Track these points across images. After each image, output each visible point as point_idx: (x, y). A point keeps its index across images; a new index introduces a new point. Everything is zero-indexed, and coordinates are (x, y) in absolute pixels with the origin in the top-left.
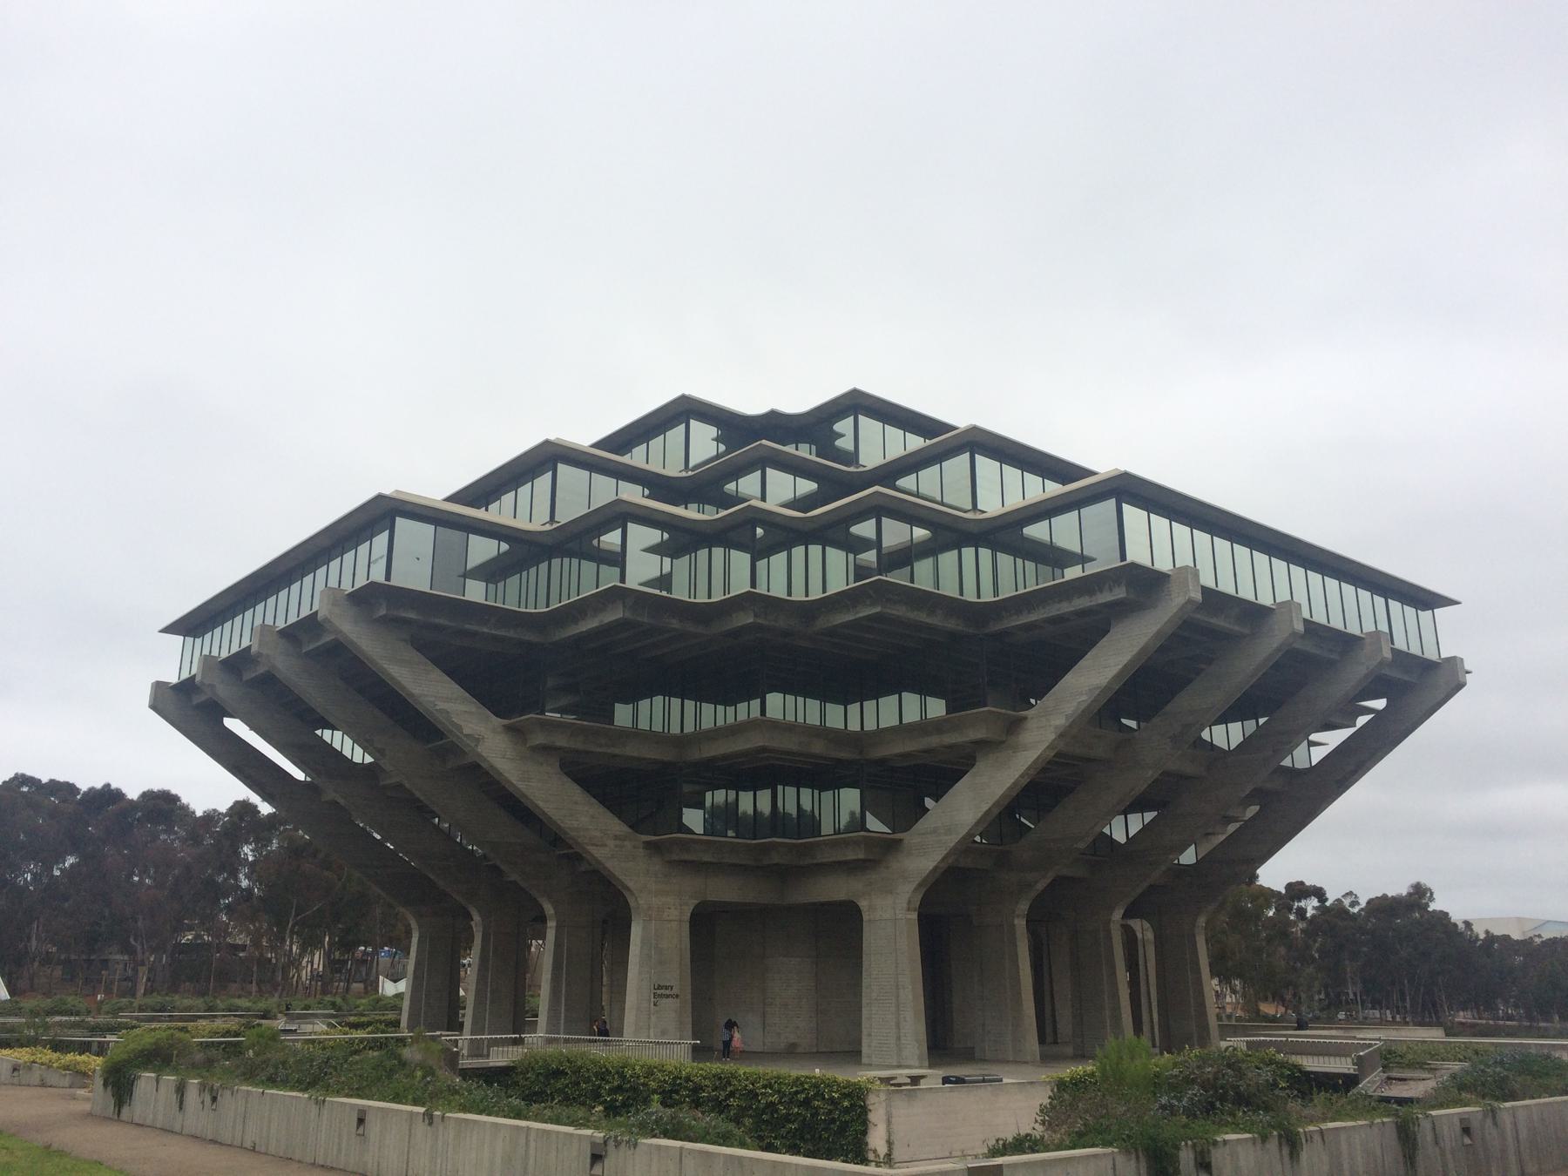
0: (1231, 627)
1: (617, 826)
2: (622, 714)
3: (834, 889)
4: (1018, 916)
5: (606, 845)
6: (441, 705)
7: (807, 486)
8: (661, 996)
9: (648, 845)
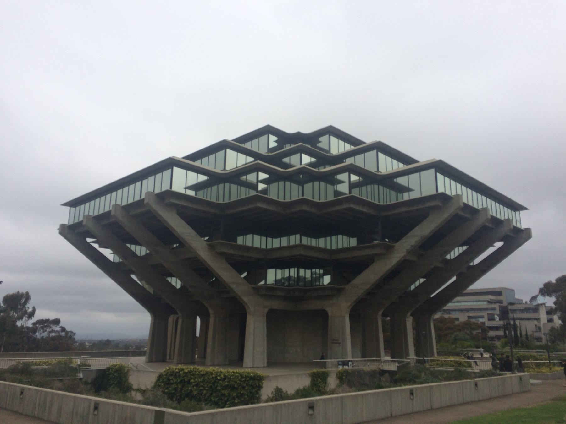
2: (240, 240)
7: (313, 160)
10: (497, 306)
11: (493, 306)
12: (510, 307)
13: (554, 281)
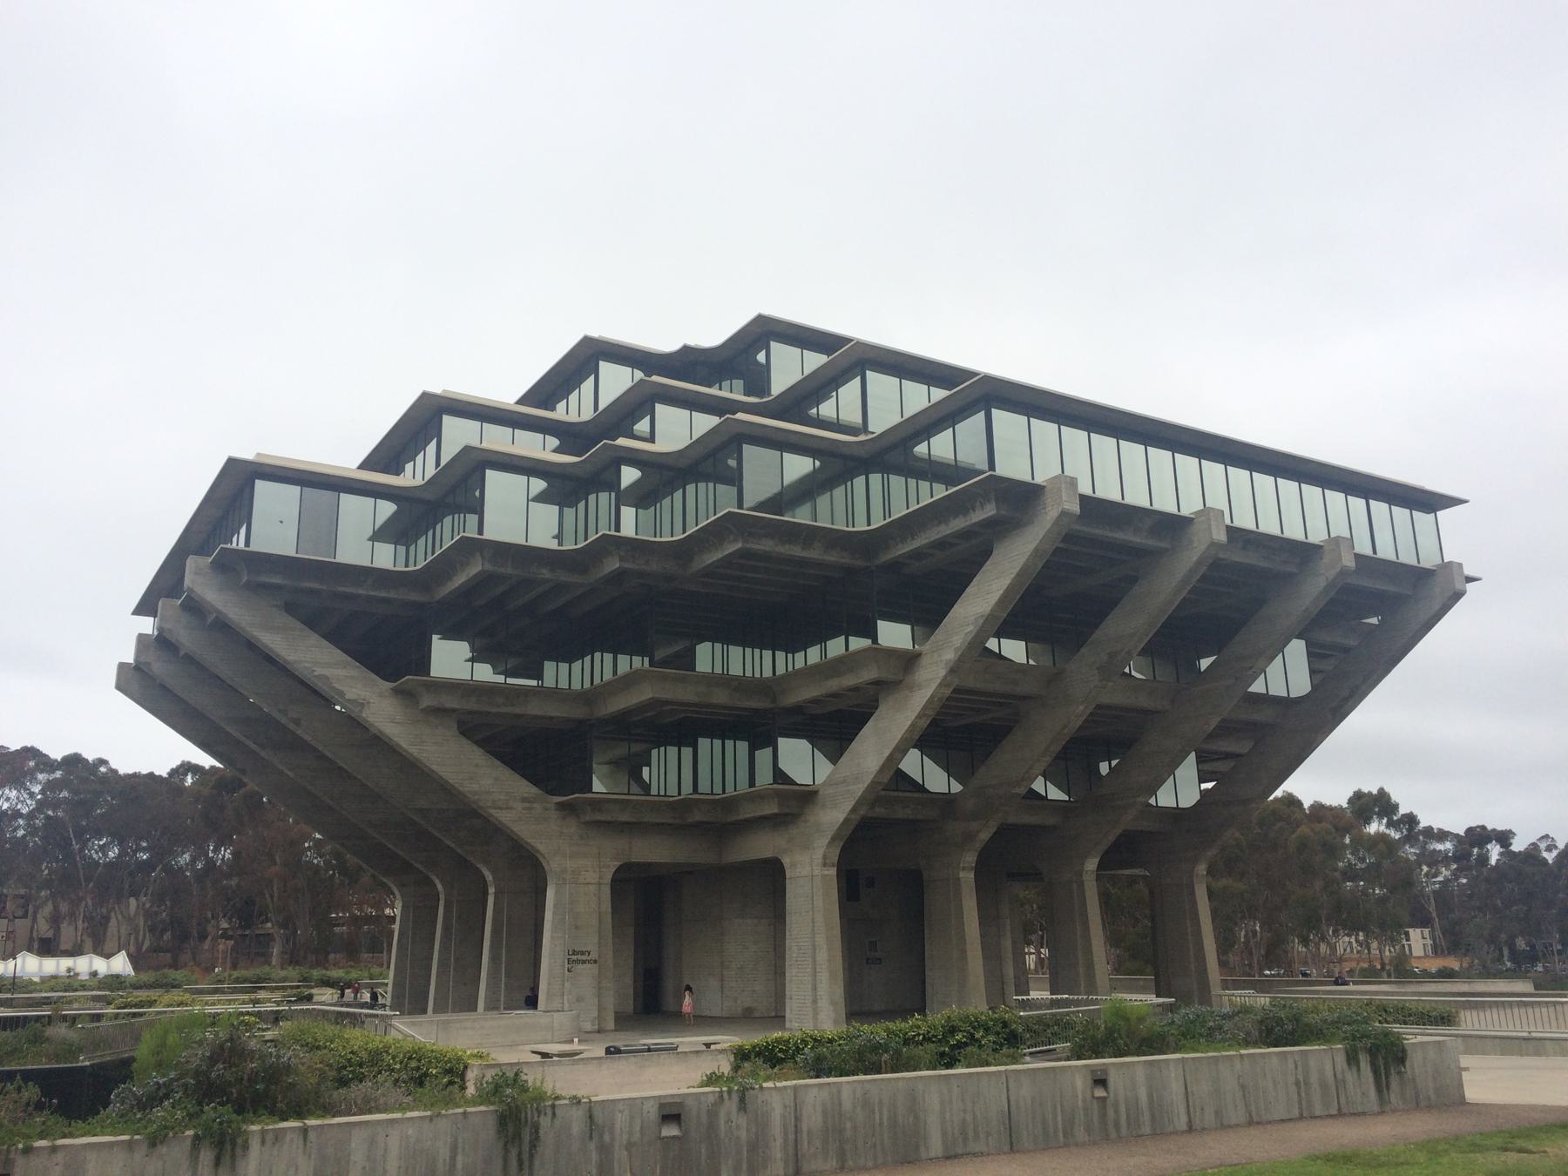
0: (1144, 541)
1: (525, 788)
3: (759, 846)
4: (964, 869)
5: (511, 808)
6: (319, 671)
8: (577, 961)
9: (561, 806)
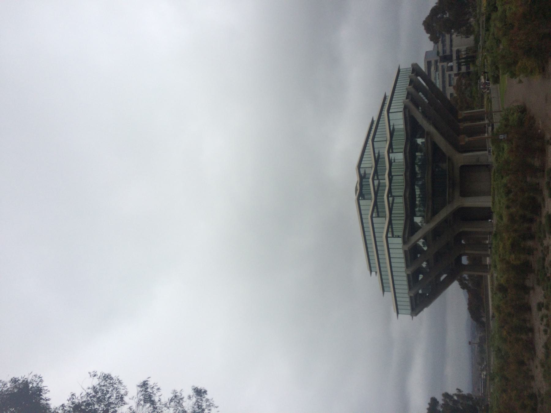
10: (440, 65)
11: (440, 68)
12: (441, 54)
13: (429, 35)
